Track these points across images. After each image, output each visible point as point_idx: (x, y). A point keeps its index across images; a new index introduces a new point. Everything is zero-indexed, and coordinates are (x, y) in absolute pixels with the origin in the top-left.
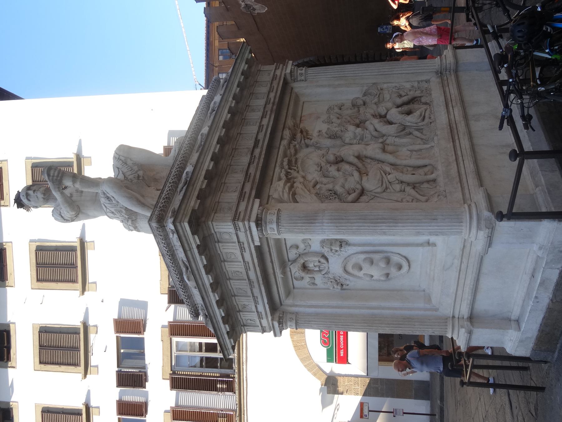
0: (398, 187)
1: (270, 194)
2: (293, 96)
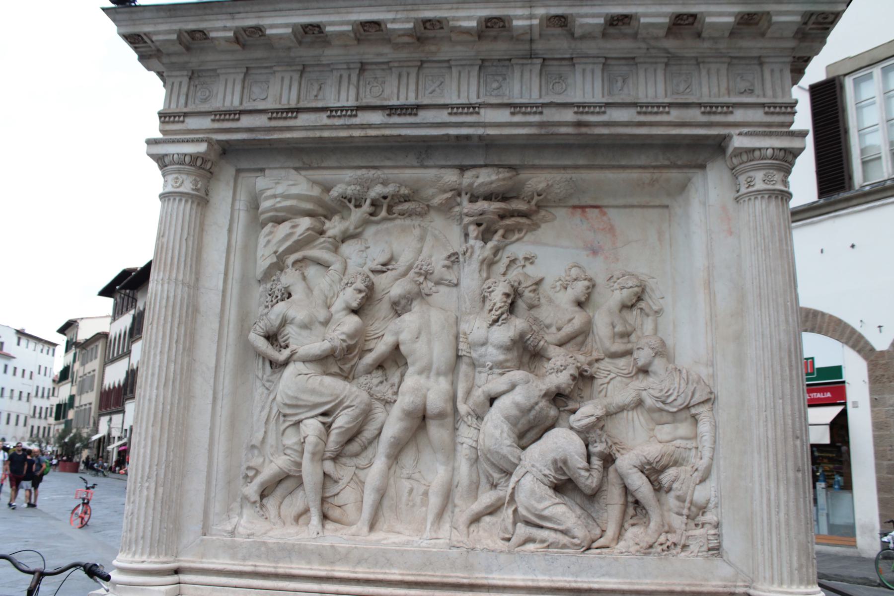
0: (291, 439)
1: (267, 172)
2: (675, 175)
